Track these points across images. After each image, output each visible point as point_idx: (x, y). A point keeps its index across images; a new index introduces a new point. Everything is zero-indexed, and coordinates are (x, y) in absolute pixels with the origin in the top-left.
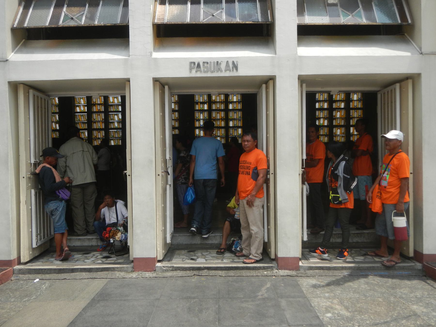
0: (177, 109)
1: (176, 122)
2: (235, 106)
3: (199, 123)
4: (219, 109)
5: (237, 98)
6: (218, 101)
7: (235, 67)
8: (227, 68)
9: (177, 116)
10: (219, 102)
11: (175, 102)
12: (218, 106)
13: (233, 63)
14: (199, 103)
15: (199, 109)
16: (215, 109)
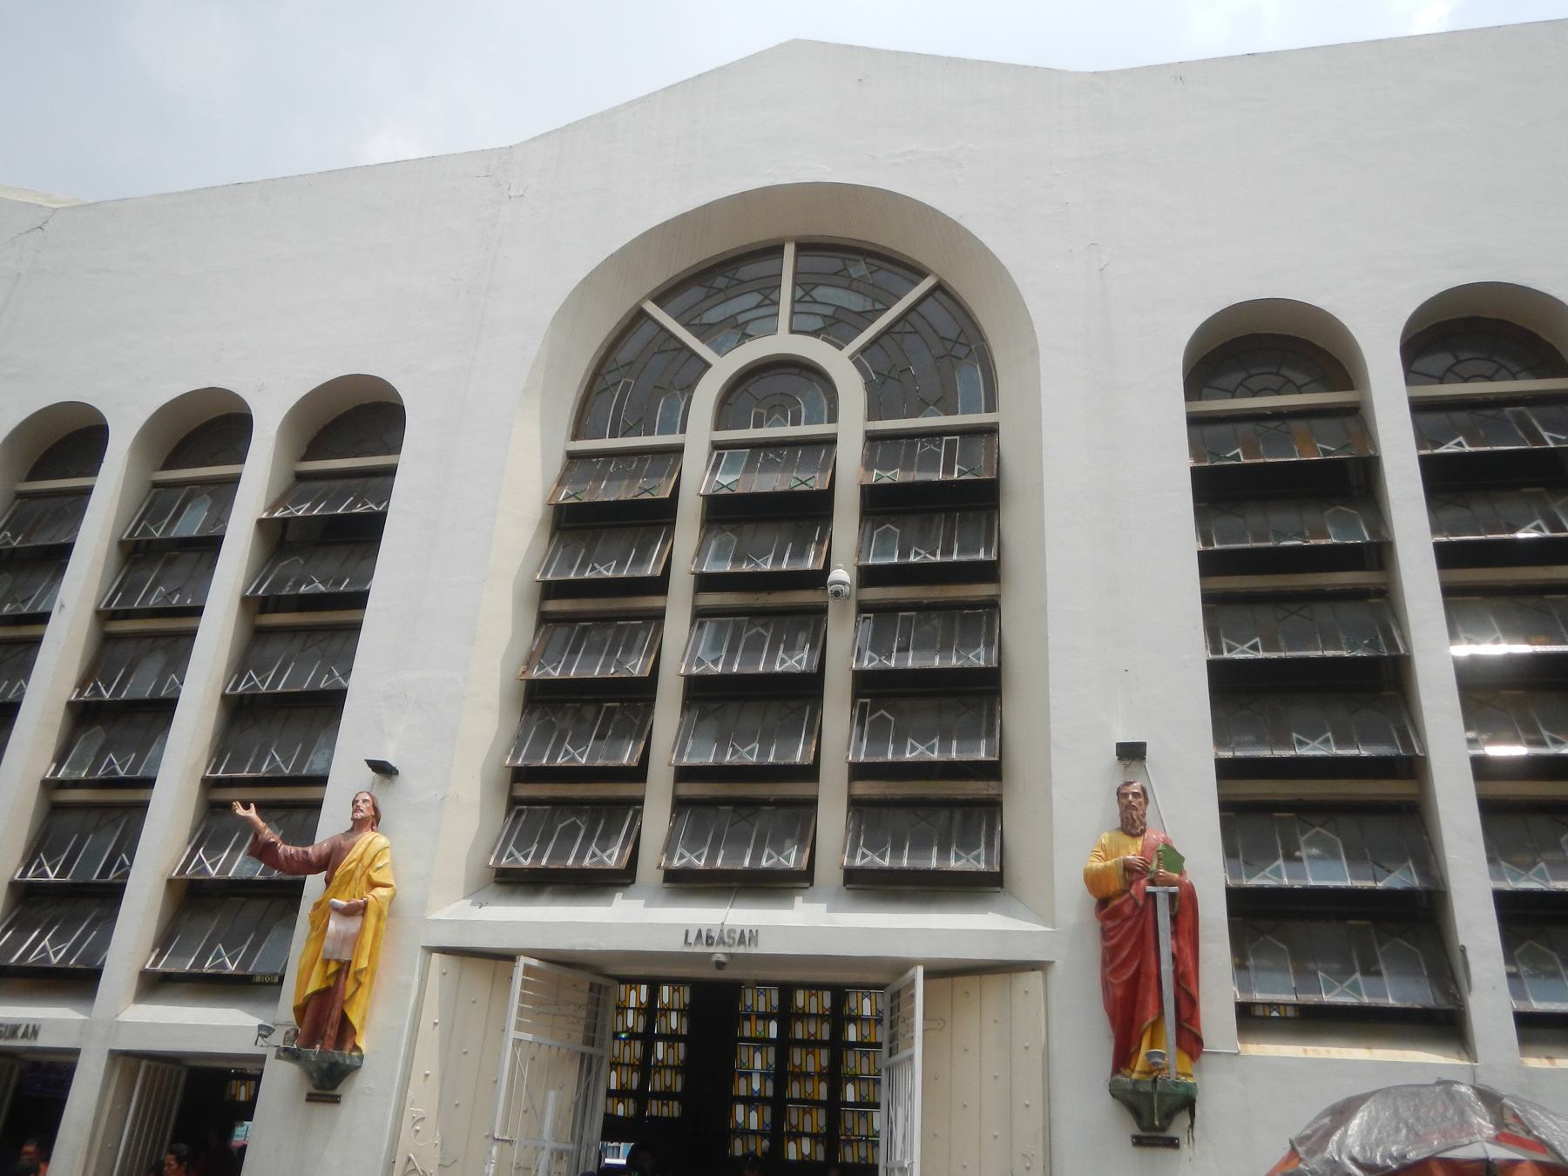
0: (684, 1032)
1: (676, 1075)
2: (866, 1032)
3: (749, 1084)
4: (816, 1041)
5: (874, 1007)
6: (814, 1011)
7: (35, 1033)
8: (25, 1035)
9: (682, 1056)
10: (816, 1016)
11: (682, 1007)
12: (812, 1029)
13: (34, 1027)
14: (753, 1017)
15: (753, 1035)
16: (801, 1037)
